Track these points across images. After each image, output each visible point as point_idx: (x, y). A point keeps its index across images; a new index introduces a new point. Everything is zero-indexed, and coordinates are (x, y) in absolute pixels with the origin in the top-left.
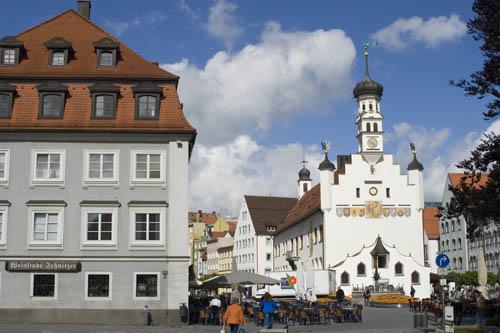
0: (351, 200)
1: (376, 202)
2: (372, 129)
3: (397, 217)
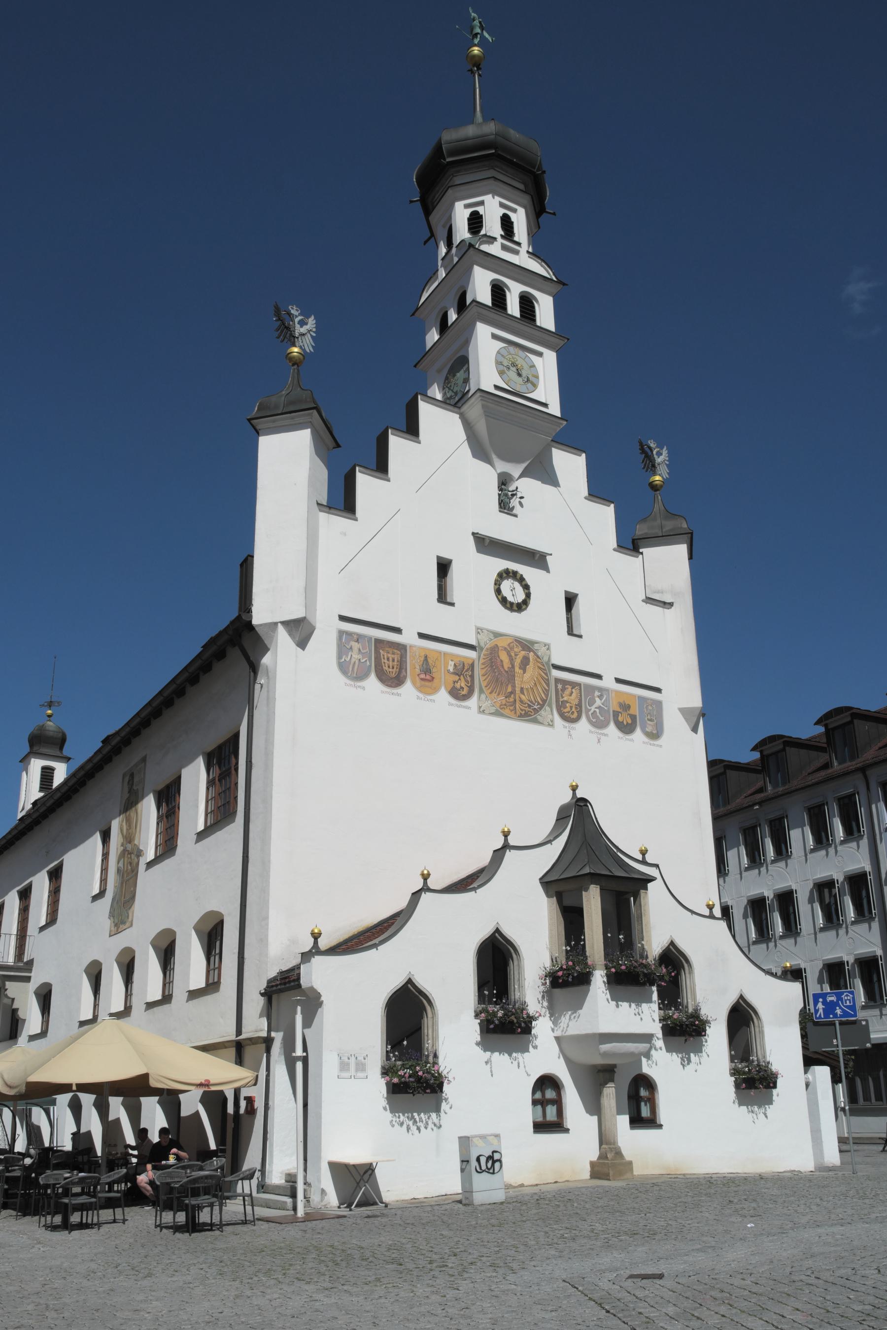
0: (414, 613)
1: (527, 645)
2: (513, 307)
3: (612, 729)
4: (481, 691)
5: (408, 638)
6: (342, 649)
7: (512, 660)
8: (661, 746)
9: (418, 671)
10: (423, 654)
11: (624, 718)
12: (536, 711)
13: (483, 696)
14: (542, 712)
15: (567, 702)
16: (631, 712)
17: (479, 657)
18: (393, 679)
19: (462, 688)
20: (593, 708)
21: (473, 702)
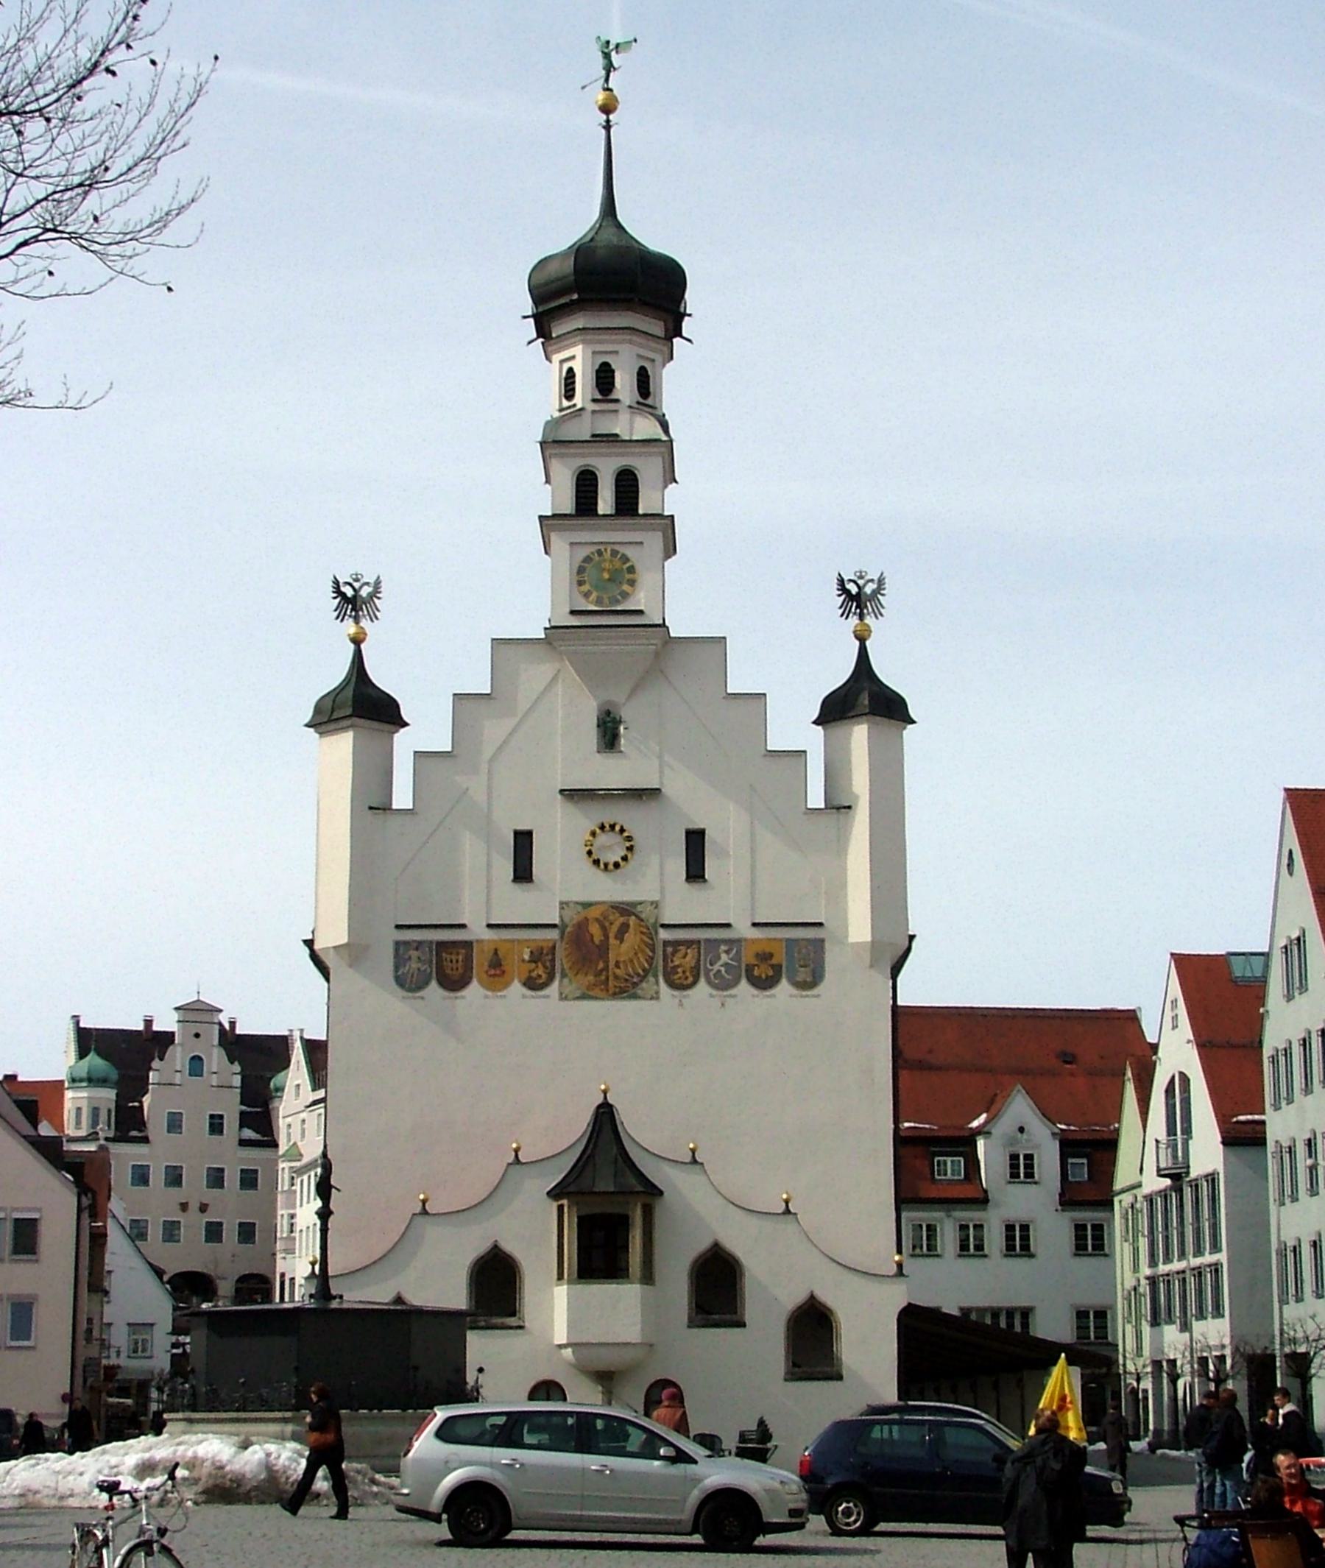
1: (625, 909)
4: (564, 975)
5: (477, 931)
6: (399, 960)
7: (605, 930)
8: (818, 996)
9: (486, 968)
10: (493, 947)
11: (762, 971)
12: (635, 985)
13: (566, 981)
14: (644, 985)
15: (678, 966)
16: (774, 961)
17: (562, 937)
18: (454, 983)
19: (540, 976)
20: (716, 967)
21: (554, 988)
